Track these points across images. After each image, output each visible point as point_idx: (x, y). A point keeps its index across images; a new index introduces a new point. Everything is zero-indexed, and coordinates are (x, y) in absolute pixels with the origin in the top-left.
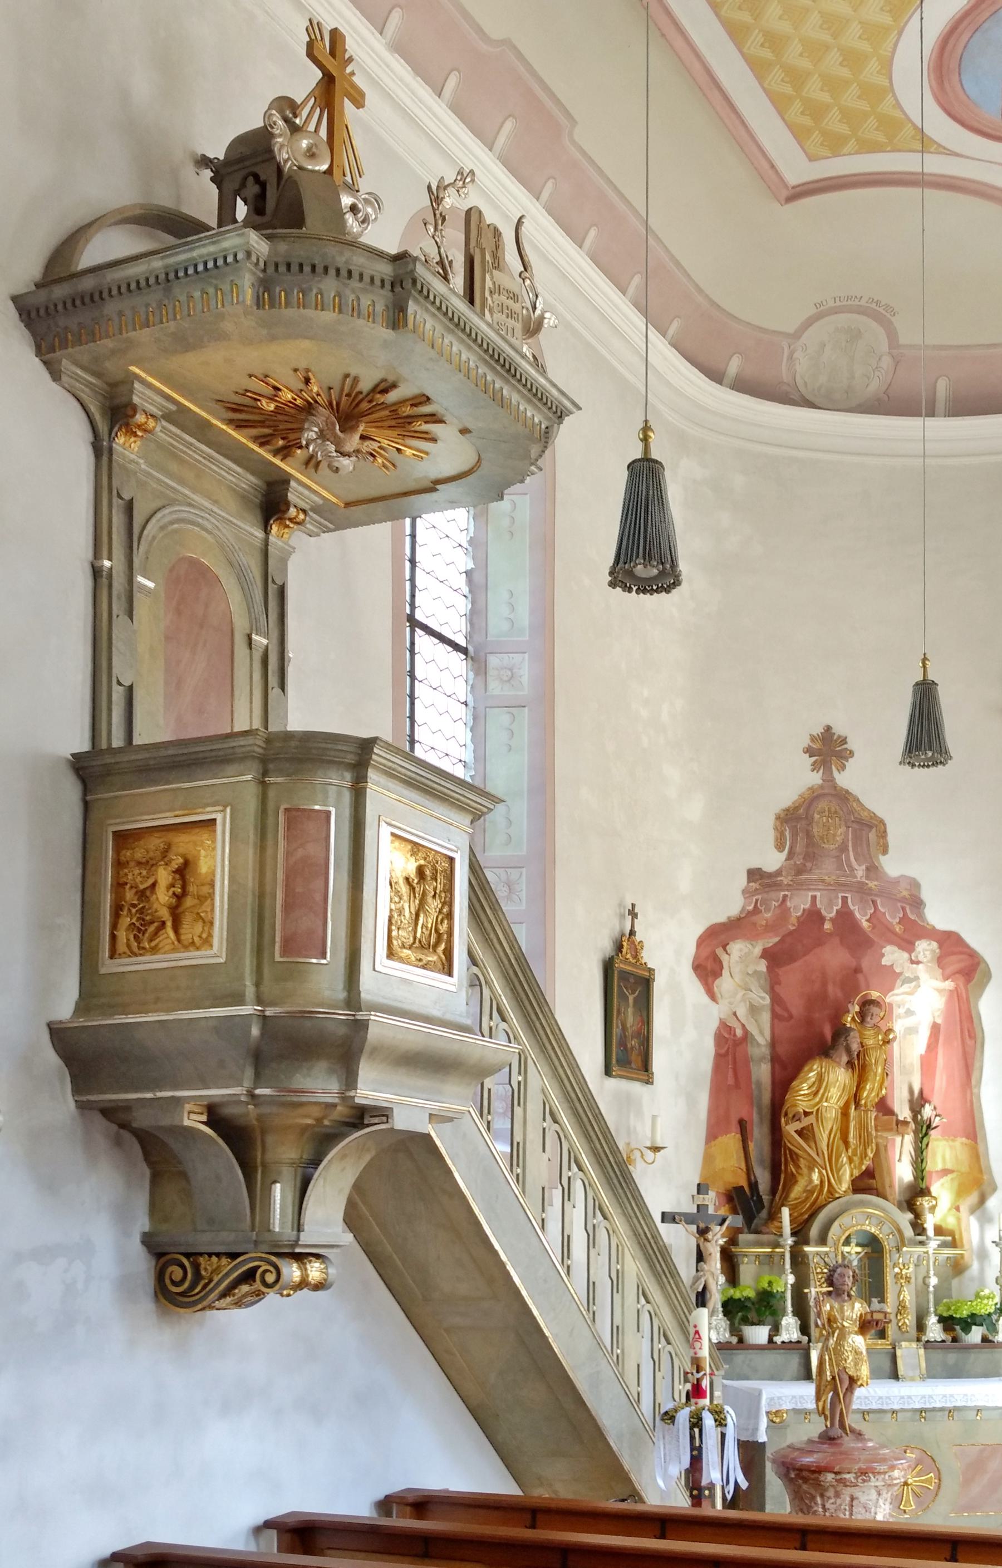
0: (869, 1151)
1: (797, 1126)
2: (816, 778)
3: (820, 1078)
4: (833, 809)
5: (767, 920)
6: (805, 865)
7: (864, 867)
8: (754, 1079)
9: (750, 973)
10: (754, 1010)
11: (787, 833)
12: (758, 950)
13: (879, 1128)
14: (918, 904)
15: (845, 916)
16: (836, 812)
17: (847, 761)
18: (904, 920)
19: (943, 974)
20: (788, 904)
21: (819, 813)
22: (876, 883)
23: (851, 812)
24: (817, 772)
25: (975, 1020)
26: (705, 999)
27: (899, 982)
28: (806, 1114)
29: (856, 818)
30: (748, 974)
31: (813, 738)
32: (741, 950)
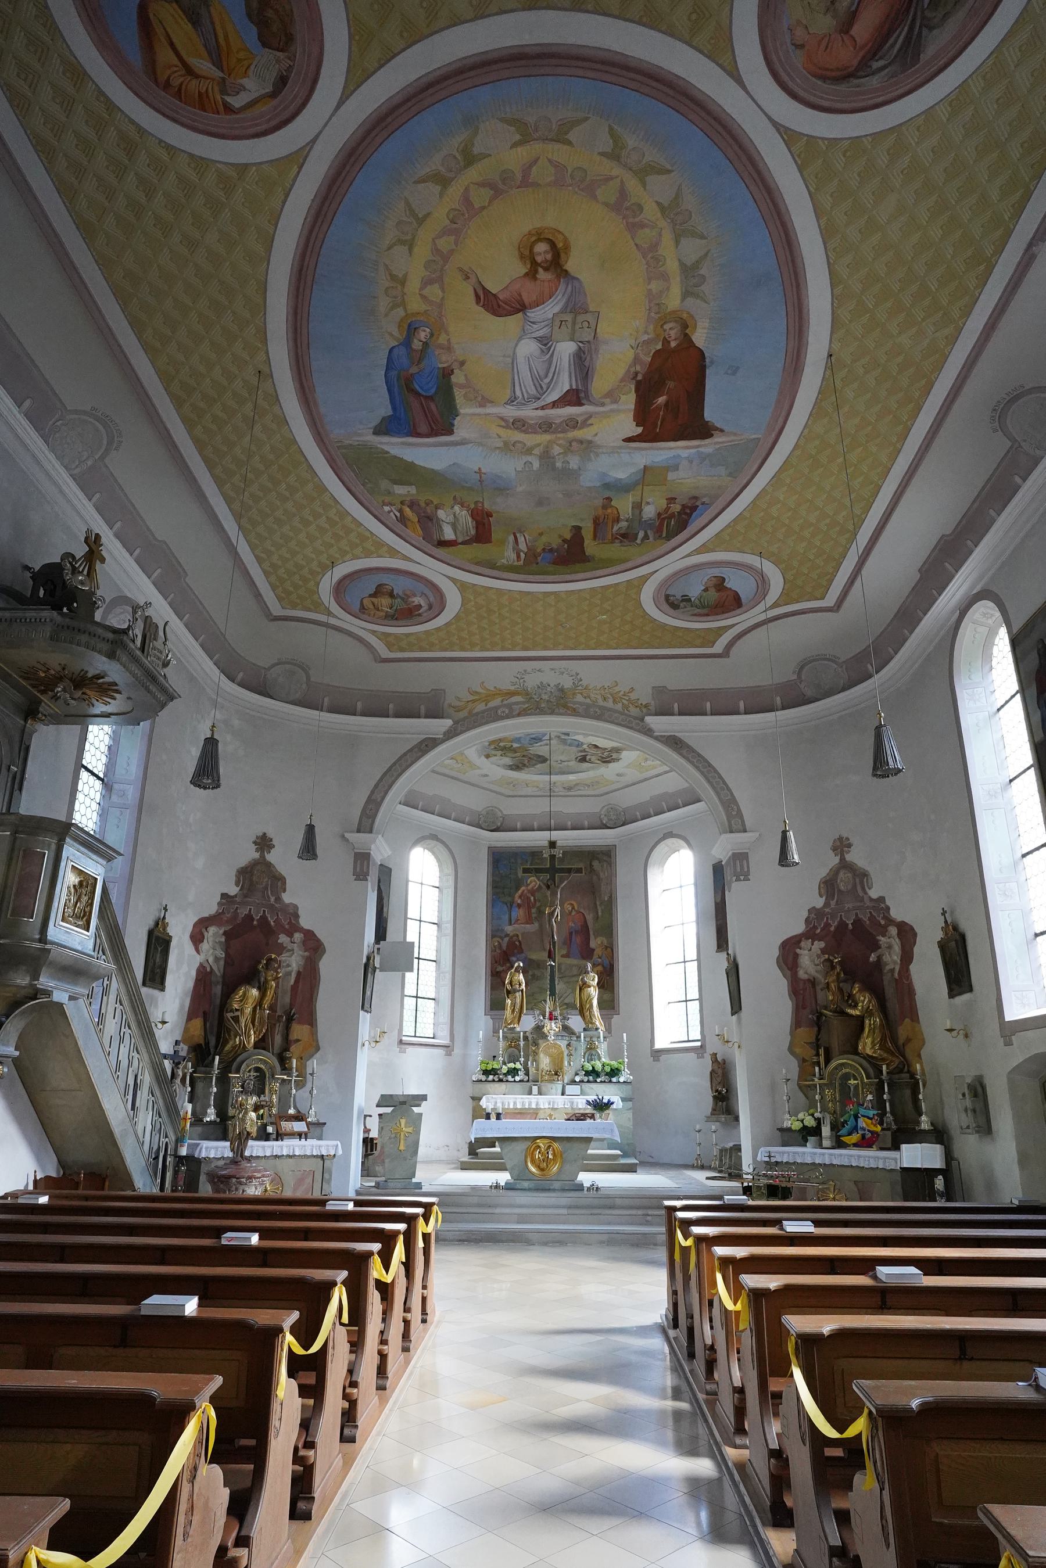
1: (232, 1014)
2: (257, 855)
3: (244, 994)
8: (213, 992)
10: (217, 959)
12: (221, 932)
14: (297, 916)
15: (264, 918)
18: (290, 923)
28: (237, 1010)
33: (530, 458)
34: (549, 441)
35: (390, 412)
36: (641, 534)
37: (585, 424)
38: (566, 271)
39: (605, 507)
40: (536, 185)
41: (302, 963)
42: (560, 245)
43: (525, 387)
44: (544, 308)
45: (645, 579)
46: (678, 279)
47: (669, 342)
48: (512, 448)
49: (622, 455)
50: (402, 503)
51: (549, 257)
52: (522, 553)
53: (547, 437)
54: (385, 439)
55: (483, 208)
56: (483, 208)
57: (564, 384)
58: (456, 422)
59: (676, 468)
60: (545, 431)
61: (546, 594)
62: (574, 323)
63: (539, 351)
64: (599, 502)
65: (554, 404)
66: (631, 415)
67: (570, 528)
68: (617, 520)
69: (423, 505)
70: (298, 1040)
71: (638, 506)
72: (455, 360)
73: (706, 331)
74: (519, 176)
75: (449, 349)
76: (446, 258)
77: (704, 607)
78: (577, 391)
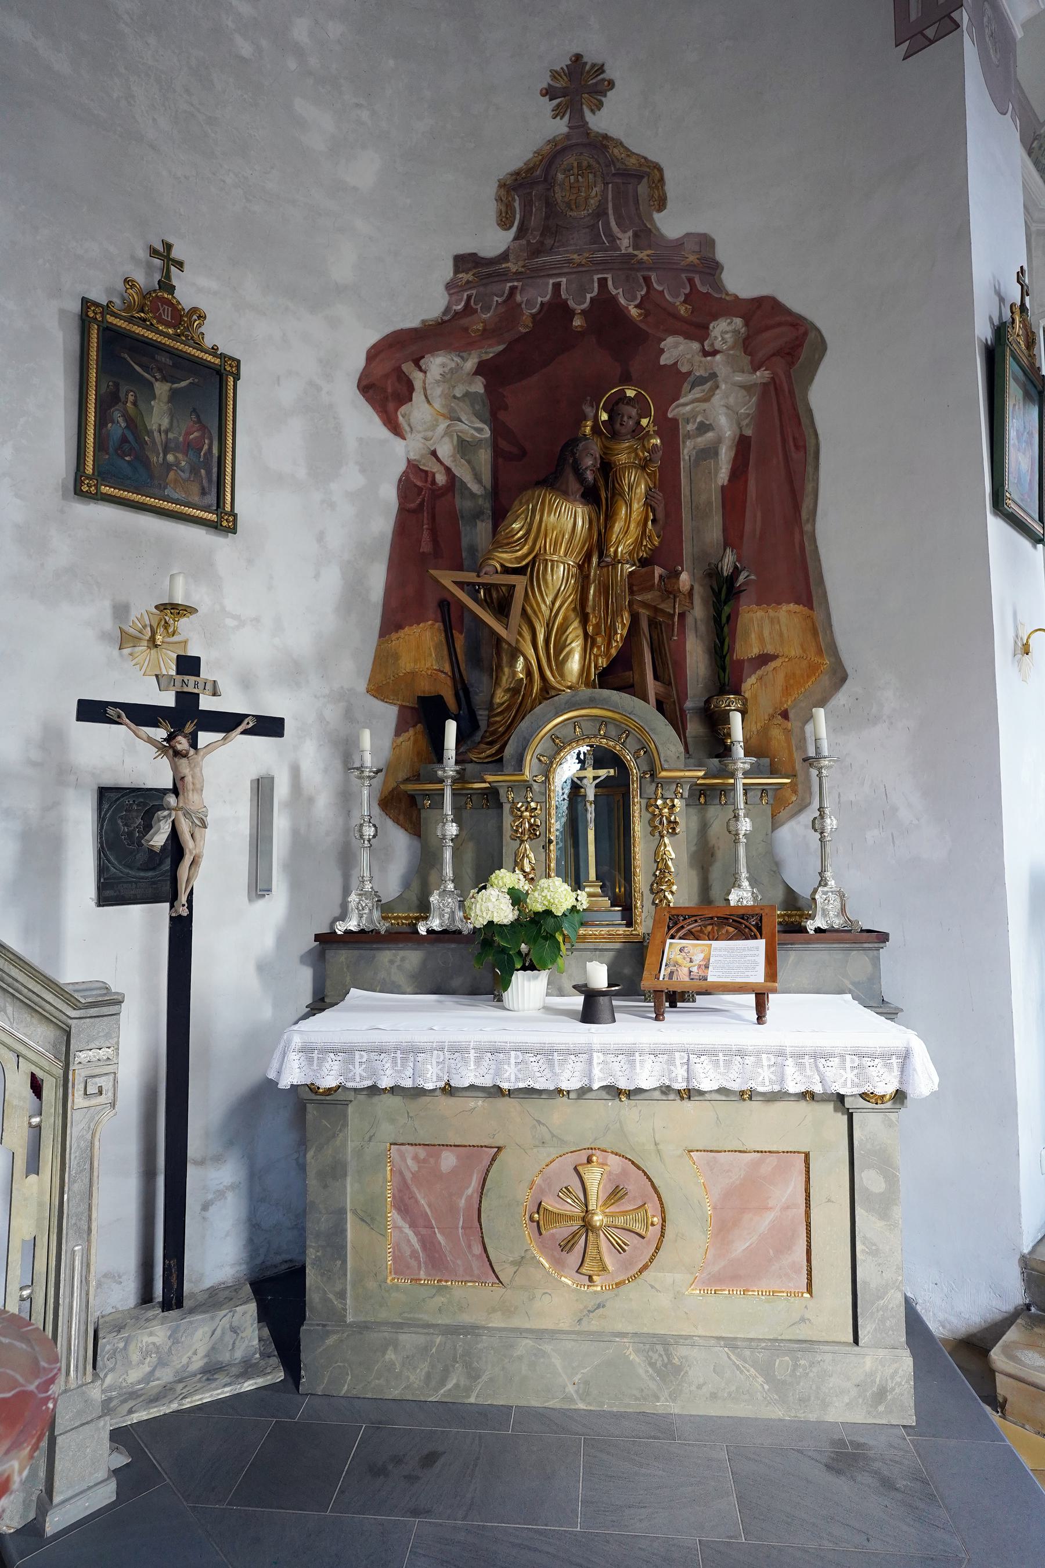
0: (619, 625)
2: (560, 127)
4: (585, 164)
5: (484, 322)
6: (542, 243)
7: (630, 233)
8: (465, 542)
9: (458, 395)
10: (464, 447)
11: (517, 205)
12: (470, 364)
13: (635, 588)
14: (711, 268)
15: (605, 305)
16: (589, 166)
17: (605, 96)
19: (752, 362)
20: (518, 298)
21: (564, 171)
22: (649, 252)
23: (612, 162)
24: (561, 119)
25: (804, 420)
26: (384, 433)
27: (686, 386)
29: (619, 169)
30: (455, 397)
31: (555, 75)
32: (443, 365)
41: (747, 406)
70: (764, 659)
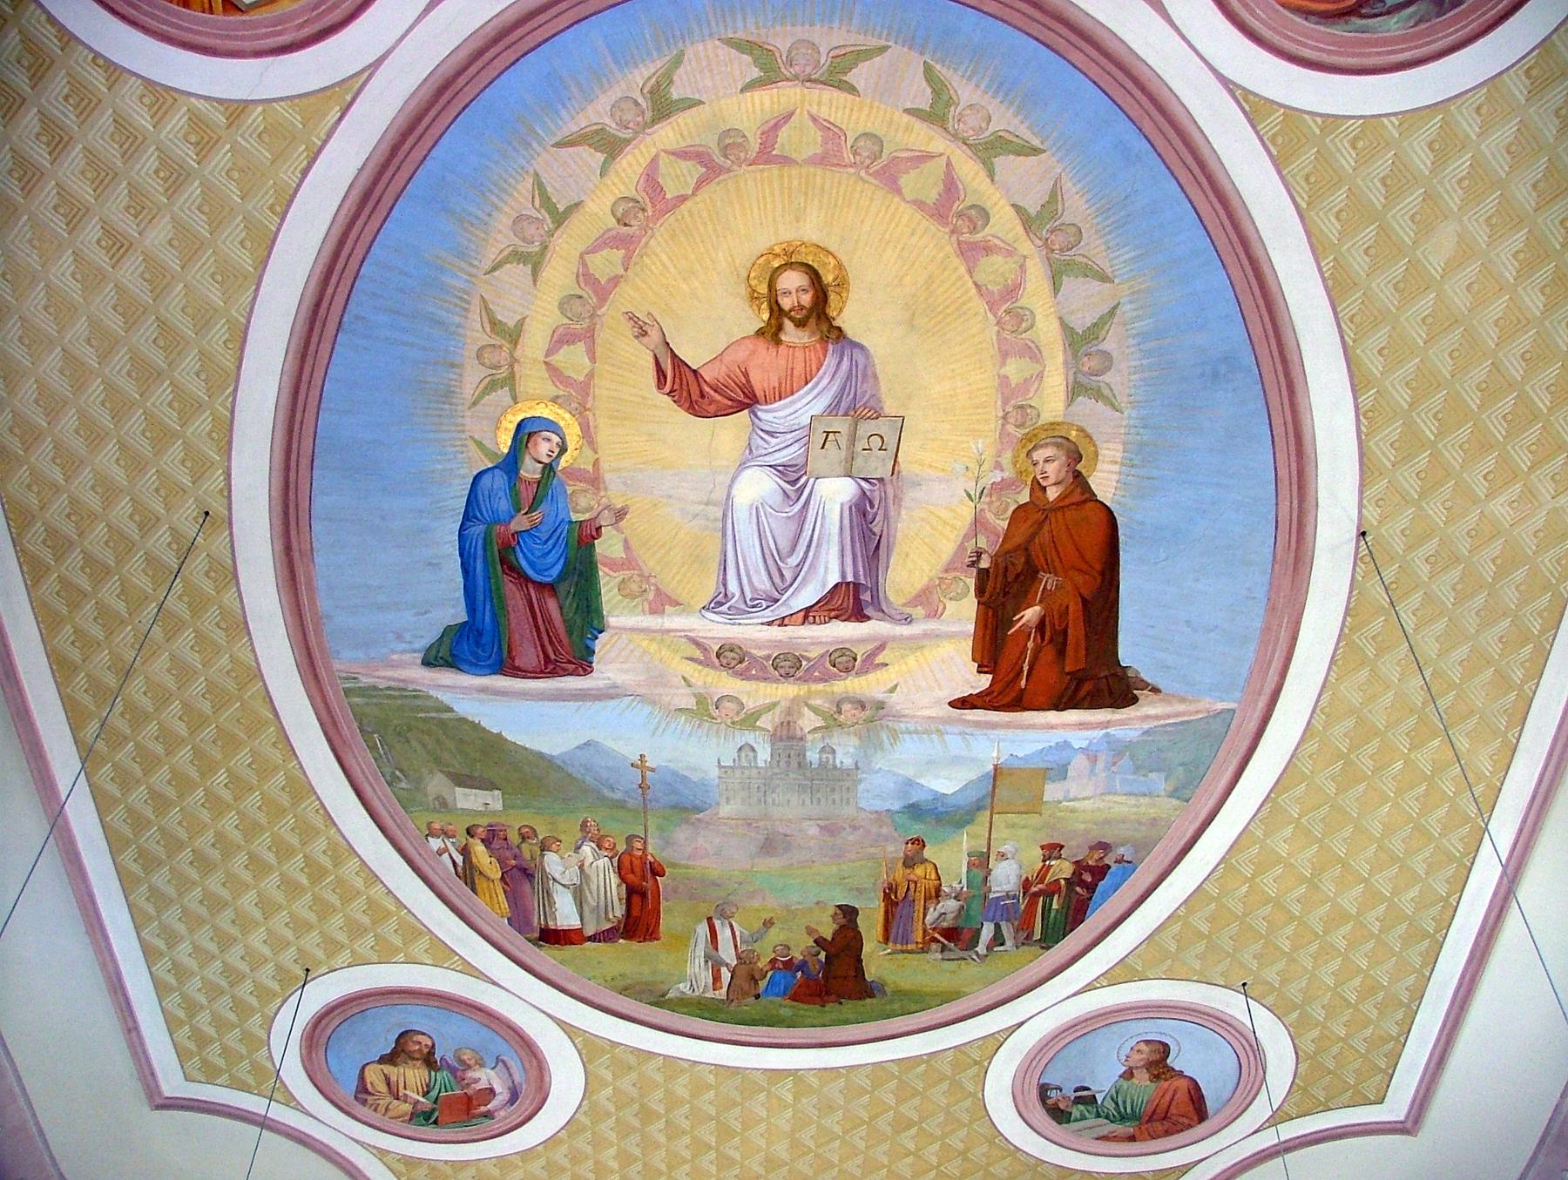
33: (749, 737)
34: (793, 700)
35: (463, 617)
36: (987, 932)
37: (871, 663)
38: (839, 329)
39: (909, 862)
40: (785, 161)
42: (828, 278)
43: (748, 575)
44: (793, 402)
45: (996, 1042)
46: (1060, 359)
47: (1044, 489)
48: (715, 713)
49: (947, 738)
50: (469, 832)
51: (806, 299)
52: (724, 970)
53: (787, 691)
54: (448, 677)
55: (683, 199)
56: (683, 199)
57: (829, 570)
58: (598, 646)
59: (1061, 772)
60: (788, 676)
61: (776, 1074)
62: (853, 439)
63: (779, 497)
64: (897, 850)
65: (807, 615)
66: (967, 645)
67: (831, 911)
68: (937, 894)
69: (514, 838)
71: (981, 862)
72: (607, 507)
73: (1116, 468)
74: (754, 145)
75: (595, 480)
76: (603, 291)
77: (1123, 1118)
78: (857, 586)
